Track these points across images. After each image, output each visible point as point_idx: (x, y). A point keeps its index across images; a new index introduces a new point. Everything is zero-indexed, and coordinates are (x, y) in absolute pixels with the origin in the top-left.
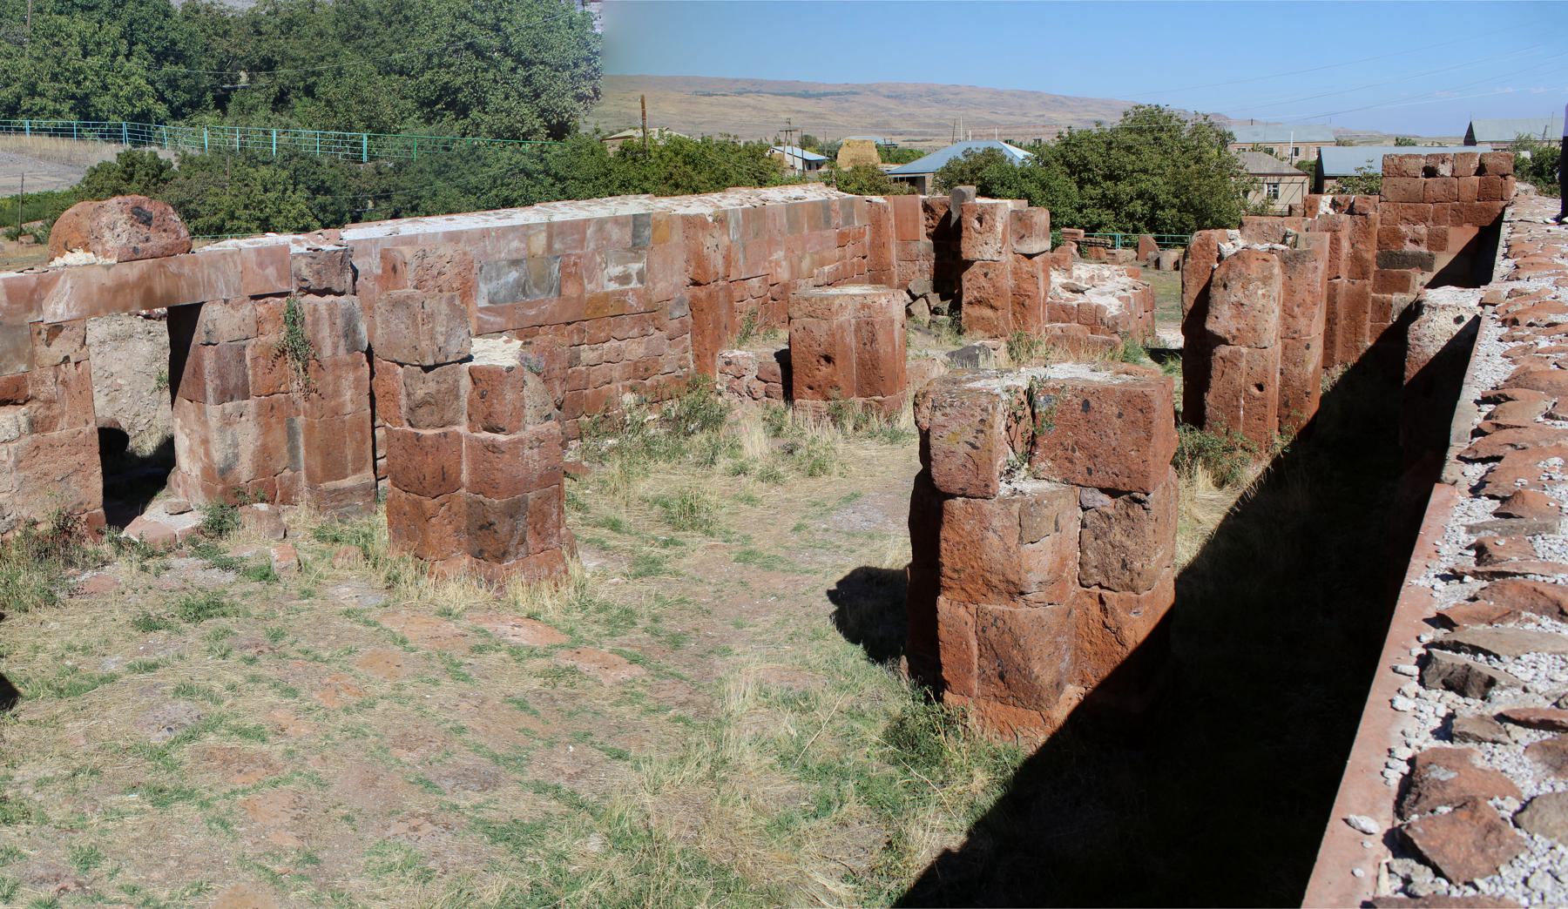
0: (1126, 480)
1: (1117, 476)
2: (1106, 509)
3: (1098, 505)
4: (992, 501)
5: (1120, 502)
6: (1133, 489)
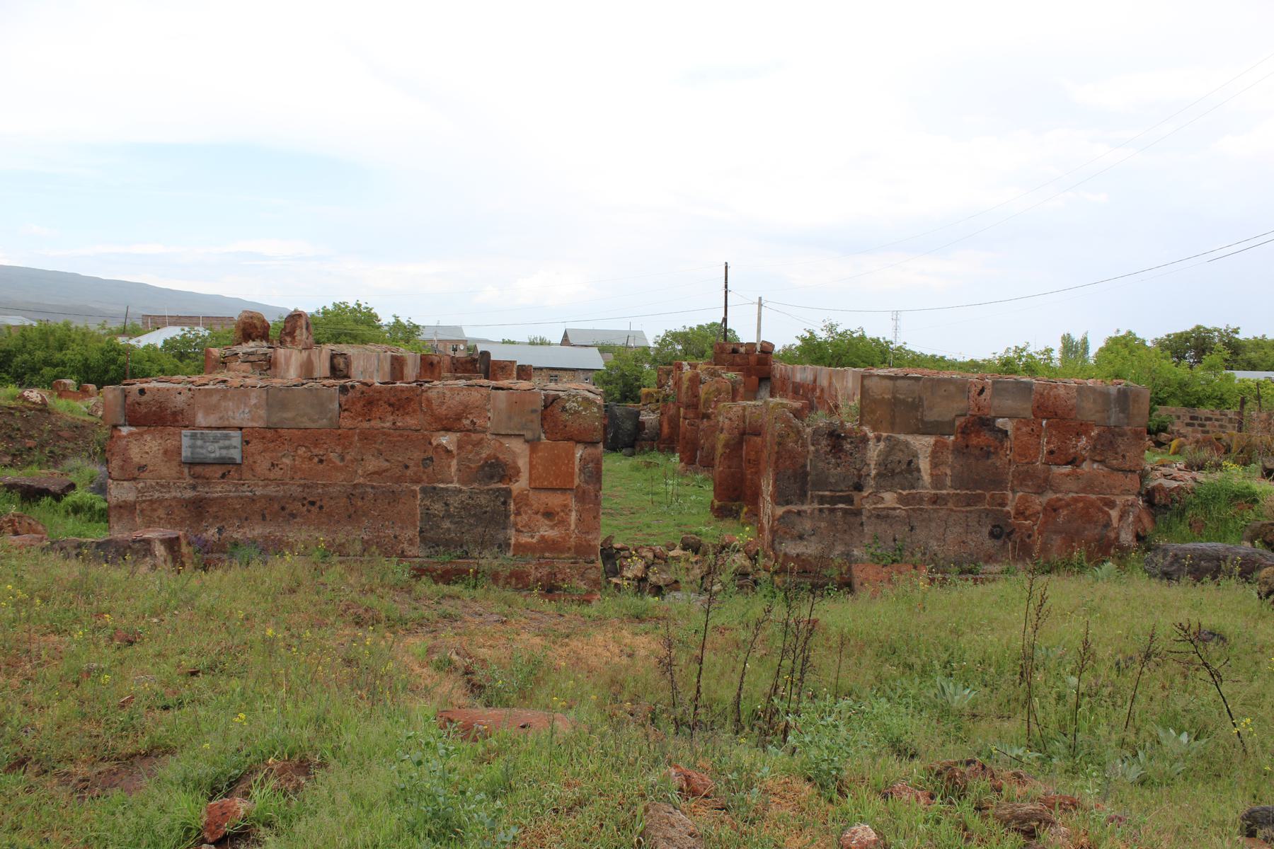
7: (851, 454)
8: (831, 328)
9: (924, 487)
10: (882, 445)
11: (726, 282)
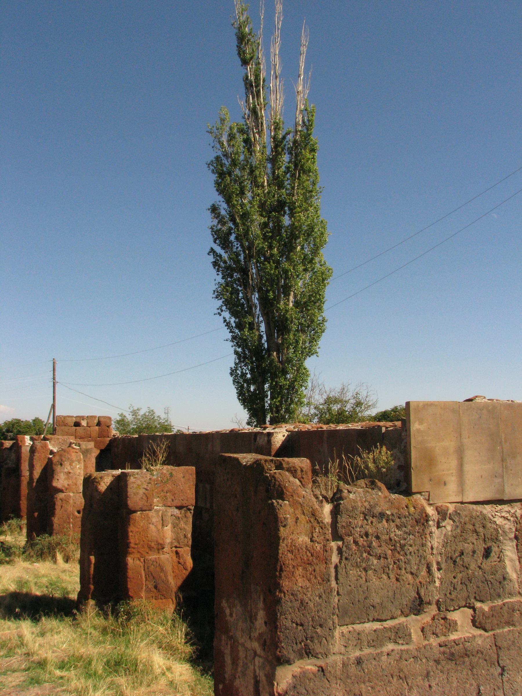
0: (186, 502)
1: (183, 500)
2: (178, 515)
3: (175, 513)
4: (152, 511)
5: (183, 511)
6: (189, 505)
7: (402, 547)
8: (134, 413)
9: (511, 594)
10: (448, 525)
11: (54, 375)
